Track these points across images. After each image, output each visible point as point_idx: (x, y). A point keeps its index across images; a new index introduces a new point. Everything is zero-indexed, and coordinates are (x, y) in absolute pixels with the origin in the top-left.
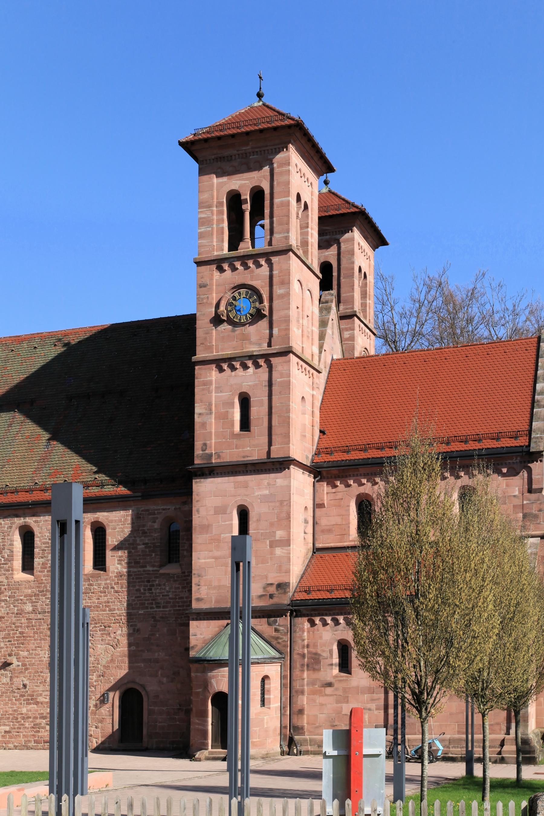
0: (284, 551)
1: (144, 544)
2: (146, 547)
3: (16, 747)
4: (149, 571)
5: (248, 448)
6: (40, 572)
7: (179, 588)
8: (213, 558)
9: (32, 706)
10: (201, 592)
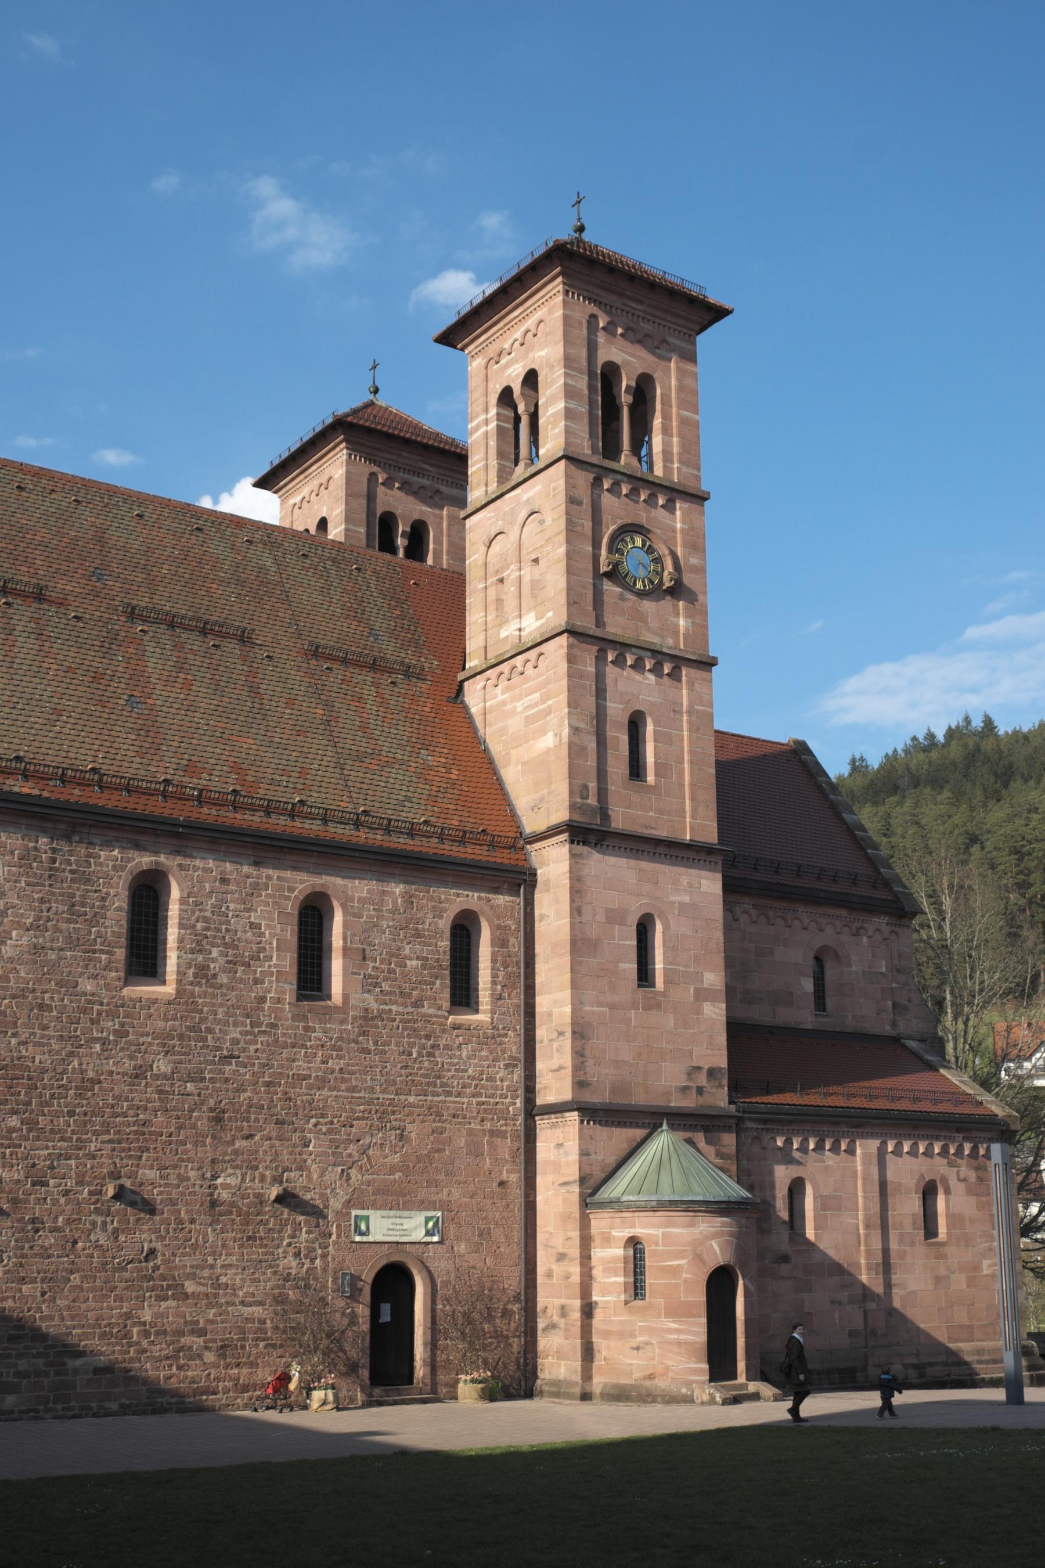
0: (716, 1010)
1: (418, 958)
2: (424, 967)
3: (124, 1410)
4: (430, 1016)
5: (652, 814)
6: (191, 984)
7: (487, 1058)
8: (607, 1005)
9: (171, 1303)
10: (587, 1069)
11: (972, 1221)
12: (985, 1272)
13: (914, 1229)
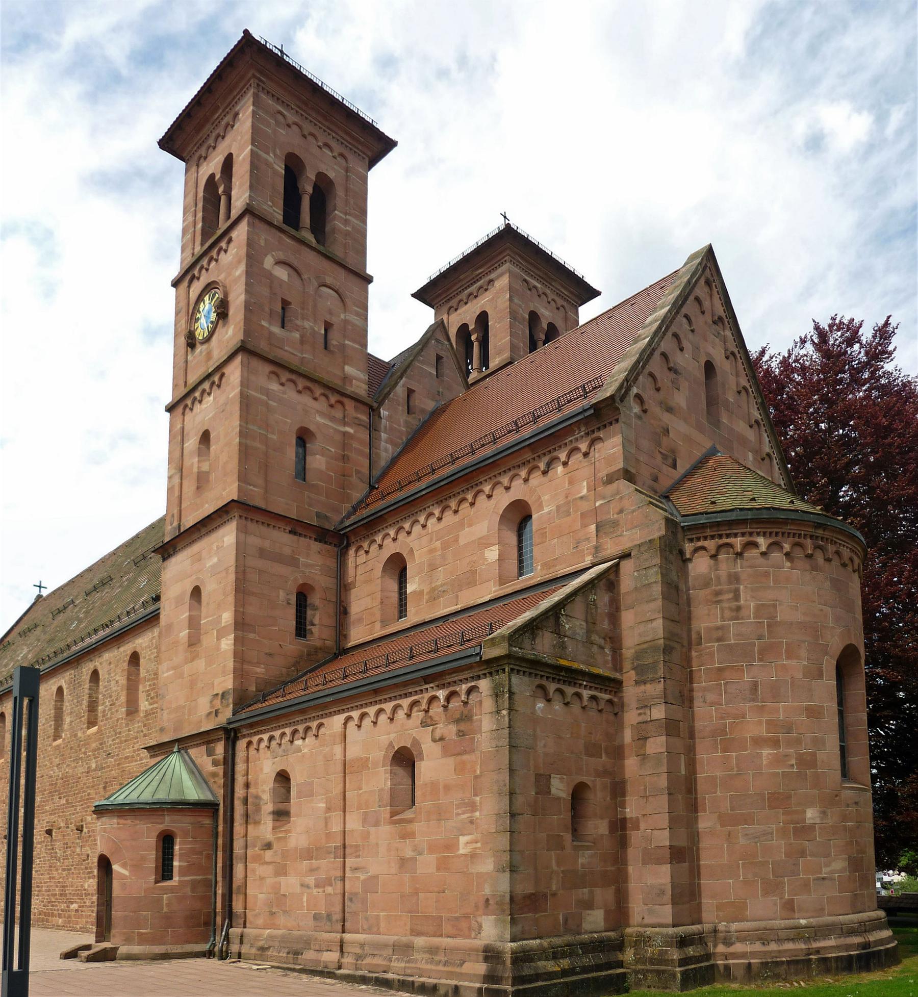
11: (447, 788)
12: (462, 851)
13: (380, 806)
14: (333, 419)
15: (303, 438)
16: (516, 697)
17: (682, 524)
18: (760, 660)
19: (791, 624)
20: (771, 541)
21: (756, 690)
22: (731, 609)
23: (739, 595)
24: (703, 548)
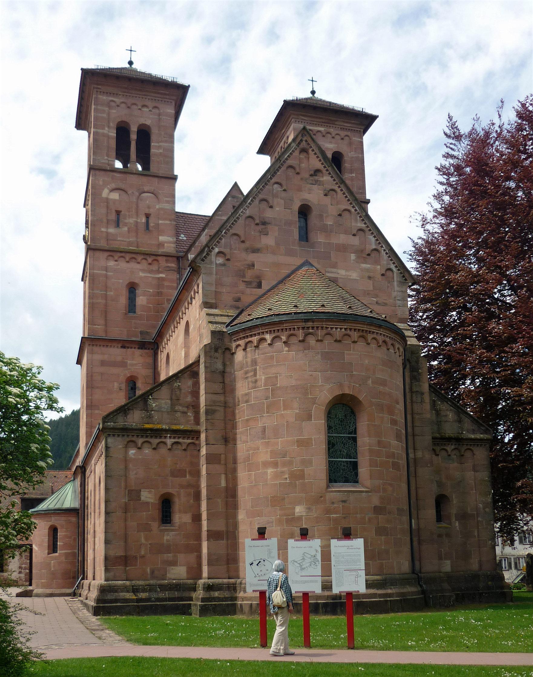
14: (151, 272)
15: (132, 288)
16: (111, 450)
17: (229, 332)
18: (268, 412)
19: (287, 387)
20: (274, 335)
21: (265, 431)
22: (252, 382)
23: (257, 372)
24: (250, 342)
